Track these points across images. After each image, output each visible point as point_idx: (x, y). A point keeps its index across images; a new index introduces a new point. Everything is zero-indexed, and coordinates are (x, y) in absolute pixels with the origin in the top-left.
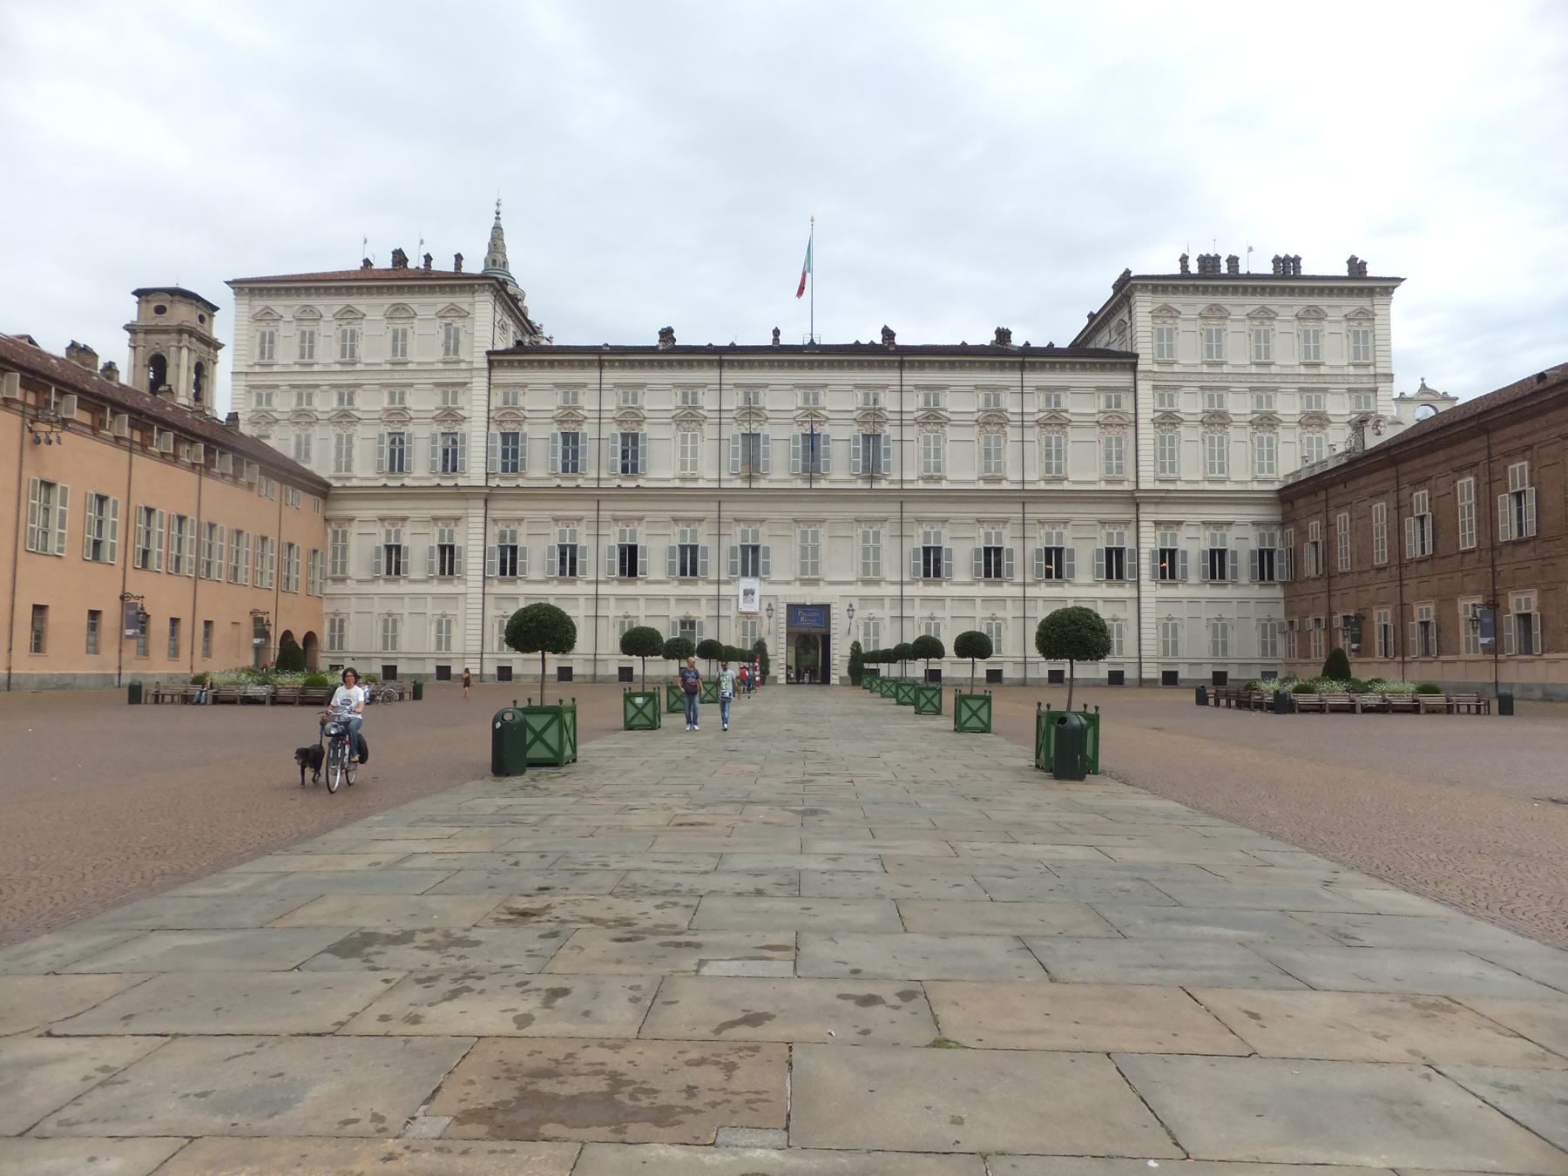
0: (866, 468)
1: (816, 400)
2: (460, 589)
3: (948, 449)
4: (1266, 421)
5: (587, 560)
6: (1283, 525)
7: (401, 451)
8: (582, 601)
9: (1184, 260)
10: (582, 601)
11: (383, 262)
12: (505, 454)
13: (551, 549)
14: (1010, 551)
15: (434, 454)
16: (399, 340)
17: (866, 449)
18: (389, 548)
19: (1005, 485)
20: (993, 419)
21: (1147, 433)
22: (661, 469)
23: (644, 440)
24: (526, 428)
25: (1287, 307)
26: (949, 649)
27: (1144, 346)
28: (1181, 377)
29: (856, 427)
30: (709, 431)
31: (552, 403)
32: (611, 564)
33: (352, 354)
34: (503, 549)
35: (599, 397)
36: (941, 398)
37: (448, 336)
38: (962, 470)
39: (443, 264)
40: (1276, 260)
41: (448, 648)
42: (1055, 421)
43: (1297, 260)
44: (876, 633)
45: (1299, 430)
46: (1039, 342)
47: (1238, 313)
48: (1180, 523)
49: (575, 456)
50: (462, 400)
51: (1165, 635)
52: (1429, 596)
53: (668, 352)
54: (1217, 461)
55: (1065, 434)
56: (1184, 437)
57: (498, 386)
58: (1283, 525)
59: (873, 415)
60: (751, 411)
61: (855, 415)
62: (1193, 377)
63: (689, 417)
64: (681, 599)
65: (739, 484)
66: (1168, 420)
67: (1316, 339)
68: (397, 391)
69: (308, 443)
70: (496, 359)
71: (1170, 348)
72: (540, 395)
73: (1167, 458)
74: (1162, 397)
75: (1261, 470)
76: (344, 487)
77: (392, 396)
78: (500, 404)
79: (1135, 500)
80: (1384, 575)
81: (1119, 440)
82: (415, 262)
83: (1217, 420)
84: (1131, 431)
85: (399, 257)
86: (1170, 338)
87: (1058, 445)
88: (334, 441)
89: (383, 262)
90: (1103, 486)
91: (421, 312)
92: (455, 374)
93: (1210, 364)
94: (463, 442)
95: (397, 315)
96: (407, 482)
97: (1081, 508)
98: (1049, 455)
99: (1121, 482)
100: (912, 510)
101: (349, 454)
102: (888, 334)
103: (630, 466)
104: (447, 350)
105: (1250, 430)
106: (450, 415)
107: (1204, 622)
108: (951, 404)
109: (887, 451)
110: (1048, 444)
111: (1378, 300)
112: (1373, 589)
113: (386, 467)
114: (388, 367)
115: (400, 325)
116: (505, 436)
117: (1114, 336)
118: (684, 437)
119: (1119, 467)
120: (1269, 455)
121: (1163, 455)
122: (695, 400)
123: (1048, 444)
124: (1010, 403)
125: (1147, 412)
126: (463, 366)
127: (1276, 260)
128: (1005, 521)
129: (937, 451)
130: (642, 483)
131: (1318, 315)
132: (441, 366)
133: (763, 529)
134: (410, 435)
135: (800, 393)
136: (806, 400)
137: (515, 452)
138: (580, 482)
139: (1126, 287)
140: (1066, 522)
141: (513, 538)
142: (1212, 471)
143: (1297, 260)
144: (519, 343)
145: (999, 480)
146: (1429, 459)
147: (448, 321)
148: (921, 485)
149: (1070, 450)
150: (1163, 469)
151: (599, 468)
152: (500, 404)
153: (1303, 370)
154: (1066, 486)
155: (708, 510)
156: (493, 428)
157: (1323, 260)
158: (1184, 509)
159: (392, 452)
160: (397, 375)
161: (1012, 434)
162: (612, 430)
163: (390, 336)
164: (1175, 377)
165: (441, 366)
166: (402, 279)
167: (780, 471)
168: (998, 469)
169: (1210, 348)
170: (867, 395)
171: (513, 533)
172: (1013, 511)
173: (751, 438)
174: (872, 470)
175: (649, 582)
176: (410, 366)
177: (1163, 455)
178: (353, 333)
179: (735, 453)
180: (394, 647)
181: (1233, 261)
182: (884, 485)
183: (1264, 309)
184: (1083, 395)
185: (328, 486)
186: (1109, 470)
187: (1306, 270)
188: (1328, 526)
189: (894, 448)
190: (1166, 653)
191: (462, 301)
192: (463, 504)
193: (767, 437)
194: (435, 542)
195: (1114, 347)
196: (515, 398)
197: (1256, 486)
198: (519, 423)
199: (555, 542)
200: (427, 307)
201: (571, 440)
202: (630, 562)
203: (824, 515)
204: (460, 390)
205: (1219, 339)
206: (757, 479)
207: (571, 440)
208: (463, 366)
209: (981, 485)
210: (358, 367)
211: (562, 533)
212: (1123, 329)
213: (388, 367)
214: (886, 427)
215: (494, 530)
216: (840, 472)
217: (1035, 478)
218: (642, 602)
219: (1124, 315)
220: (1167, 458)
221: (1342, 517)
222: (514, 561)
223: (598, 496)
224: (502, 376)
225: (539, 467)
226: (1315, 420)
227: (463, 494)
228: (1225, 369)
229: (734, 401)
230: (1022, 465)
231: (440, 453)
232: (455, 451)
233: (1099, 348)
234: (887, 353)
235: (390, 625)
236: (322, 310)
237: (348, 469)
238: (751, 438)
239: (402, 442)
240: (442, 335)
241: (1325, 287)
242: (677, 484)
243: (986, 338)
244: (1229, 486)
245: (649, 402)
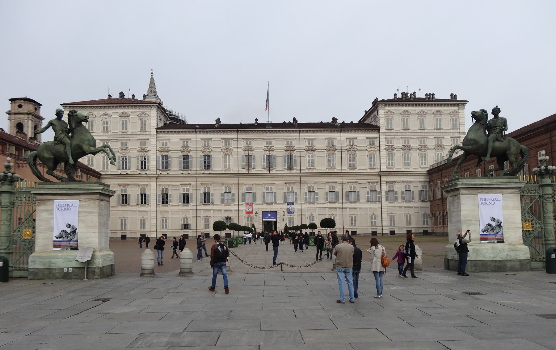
0: (288, 166)
1: (271, 143)
2: (149, 208)
3: (316, 159)
4: (423, 148)
5: (193, 198)
6: (429, 182)
7: (126, 162)
8: (191, 212)
9: (395, 95)
10: (191, 212)
11: (116, 96)
12: (163, 163)
13: (180, 194)
14: (338, 193)
15: (138, 163)
16: (124, 125)
17: (288, 159)
18: (123, 195)
19: (335, 171)
20: (331, 149)
21: (384, 153)
22: (218, 166)
23: (211, 158)
24: (170, 154)
25: (430, 110)
26: (318, 225)
27: (382, 124)
28: (395, 134)
29: (285, 152)
30: (234, 154)
31: (180, 145)
32: (201, 199)
33: (107, 129)
34: (163, 195)
35: (196, 143)
36: (314, 142)
37: (142, 123)
38: (321, 166)
39: (139, 97)
40: (426, 95)
41: (144, 228)
42: (352, 149)
43: (433, 95)
44: (293, 220)
45: (434, 151)
46: (348, 121)
47: (414, 113)
48: (395, 182)
49: (188, 163)
50: (147, 145)
51: (390, 218)
53: (219, 127)
54: (407, 161)
55: (356, 153)
56: (412, 154)
57: (160, 140)
58: (429, 182)
59: (290, 148)
60: (248, 147)
61: (284, 148)
62: (399, 134)
63: (227, 149)
64: (226, 211)
65: (245, 172)
66: (390, 148)
67: (440, 121)
68: (124, 143)
70: (159, 130)
71: (391, 124)
72: (175, 141)
73: (390, 161)
74: (388, 141)
75: (422, 164)
76: (106, 175)
77: (122, 143)
78: (161, 146)
79: (379, 175)
81: (374, 155)
82: (128, 96)
83: (407, 148)
84: (378, 152)
85: (122, 94)
86: (391, 121)
87: (353, 157)
88: (102, 159)
89: (116, 96)
90: (369, 170)
91: (132, 115)
92: (144, 136)
93: (404, 130)
94: (148, 159)
95: (123, 116)
96: (128, 172)
97: (361, 178)
98: (350, 161)
99: (375, 169)
100: (304, 179)
103: (207, 164)
104: (142, 127)
105: (418, 151)
106: (143, 149)
107: (403, 214)
108: (316, 144)
109: (295, 160)
110: (350, 157)
111: (460, 108)
113: (121, 167)
114: (120, 133)
115: (124, 119)
116: (163, 157)
117: (373, 120)
118: (225, 158)
119: (374, 164)
120: (423, 159)
122: (229, 144)
123: (350, 157)
124: (337, 144)
125: (383, 147)
126: (147, 133)
127: (426, 95)
128: (336, 183)
129: (312, 160)
130: (211, 172)
131: (440, 113)
132: (139, 133)
133: (253, 187)
134: (129, 157)
135: (265, 141)
136: (267, 144)
137: (167, 163)
138: (190, 172)
139: (376, 103)
140: (357, 183)
141: (167, 191)
142: (406, 165)
143: (433, 95)
144: (165, 124)
145: (334, 169)
147: (142, 118)
148: (307, 171)
149: (357, 158)
150: (389, 164)
151: (196, 166)
152: (161, 146)
153: (435, 131)
154: (356, 170)
155: (234, 180)
156: (159, 154)
157: (442, 94)
158: (396, 177)
159: (123, 162)
160: (124, 136)
161: (338, 153)
162: (200, 154)
163: (121, 123)
164: (392, 134)
165: (139, 133)
166: (123, 102)
167: (259, 167)
168: (333, 165)
169: (404, 125)
170: (288, 142)
171: (167, 189)
172: (338, 179)
173: (249, 156)
174: (290, 167)
175: (214, 205)
176: (128, 133)
178: (107, 122)
179: (243, 162)
180: (125, 229)
182: (294, 171)
183: (422, 111)
184: (361, 139)
185: (101, 174)
186: (371, 165)
187: (436, 97)
189: (298, 159)
190: (391, 225)
191: (146, 111)
192: (149, 180)
193: (254, 156)
194: (139, 193)
195: (373, 123)
196: (166, 144)
197: (420, 169)
198: (168, 152)
199: (181, 192)
200: (134, 113)
201: (186, 158)
202: (207, 198)
203: (274, 182)
204: (146, 141)
205: (407, 122)
206: (251, 170)
207: (186, 158)
208: (147, 133)
209: (328, 171)
210: (110, 133)
211: (184, 189)
212: (376, 117)
213: (120, 133)
214: (295, 152)
215: (160, 189)
216: (280, 167)
217: (346, 168)
218: (212, 211)
219: (375, 113)
220: (390, 161)
222: (167, 198)
223: (196, 176)
224: (161, 136)
225: (175, 166)
226: (440, 147)
227: (148, 176)
228: (410, 131)
229: (243, 144)
230: (341, 164)
231: (140, 163)
232: (145, 162)
233: (367, 124)
234: (294, 126)
235: (124, 222)
236: (96, 114)
238: (249, 156)
239: (126, 159)
240: (140, 123)
241: (442, 102)
242: (224, 172)
243: (330, 120)
244: (411, 170)
245: (212, 145)
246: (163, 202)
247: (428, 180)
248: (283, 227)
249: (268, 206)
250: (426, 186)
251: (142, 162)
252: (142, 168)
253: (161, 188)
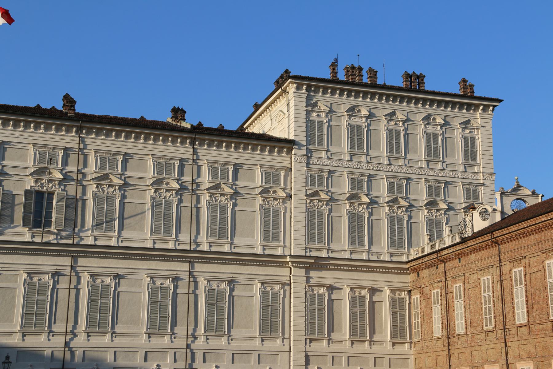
43: (421, 78)
46: (210, 123)
52: (529, 357)
80: (492, 336)
102: (69, 101)
112: (484, 348)
121: (313, 228)
143: (421, 78)
146: (523, 242)
177: (313, 228)
181: (373, 73)
188: (446, 293)
221: (457, 286)
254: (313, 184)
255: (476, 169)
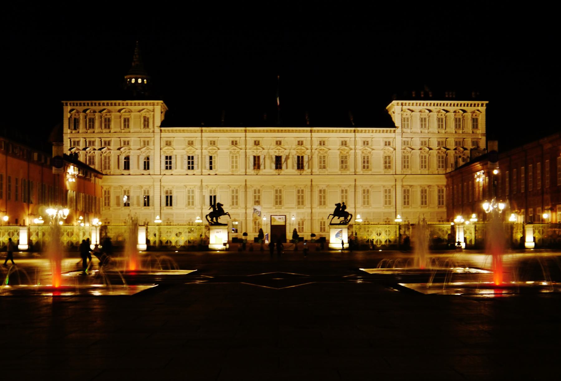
69: (93, 159)
78: (165, 144)
98: (364, 162)
101: (109, 163)
110: (364, 159)
121: (405, 162)
129: (324, 161)
177: (405, 162)
219: (393, 110)
232: (148, 163)
237: (109, 168)
246: (167, 205)
247: (445, 183)
248: (292, 231)
249: (277, 210)
250: (443, 190)
251: (145, 162)
252: (145, 169)
253: (165, 189)
254: (404, 144)
255: (478, 132)
